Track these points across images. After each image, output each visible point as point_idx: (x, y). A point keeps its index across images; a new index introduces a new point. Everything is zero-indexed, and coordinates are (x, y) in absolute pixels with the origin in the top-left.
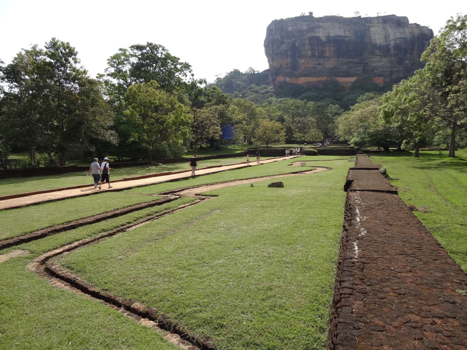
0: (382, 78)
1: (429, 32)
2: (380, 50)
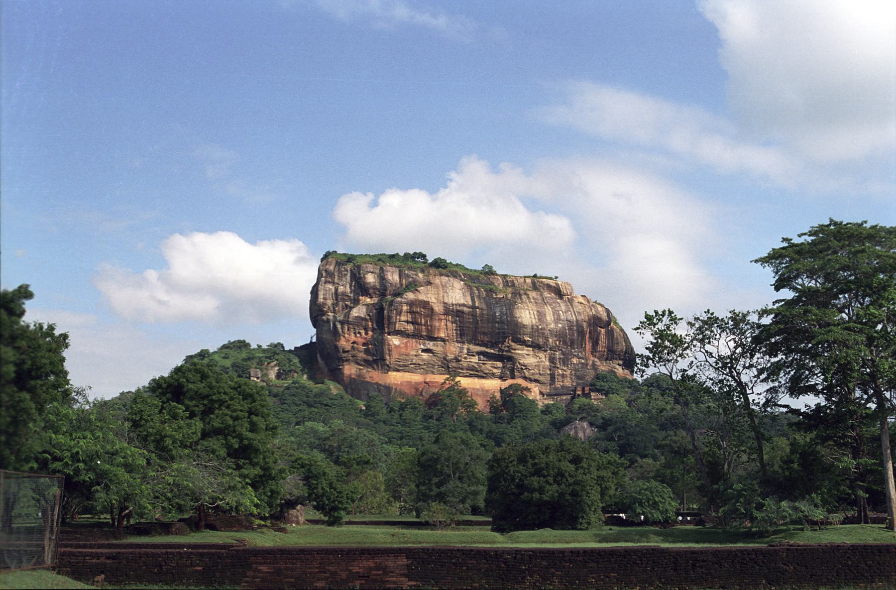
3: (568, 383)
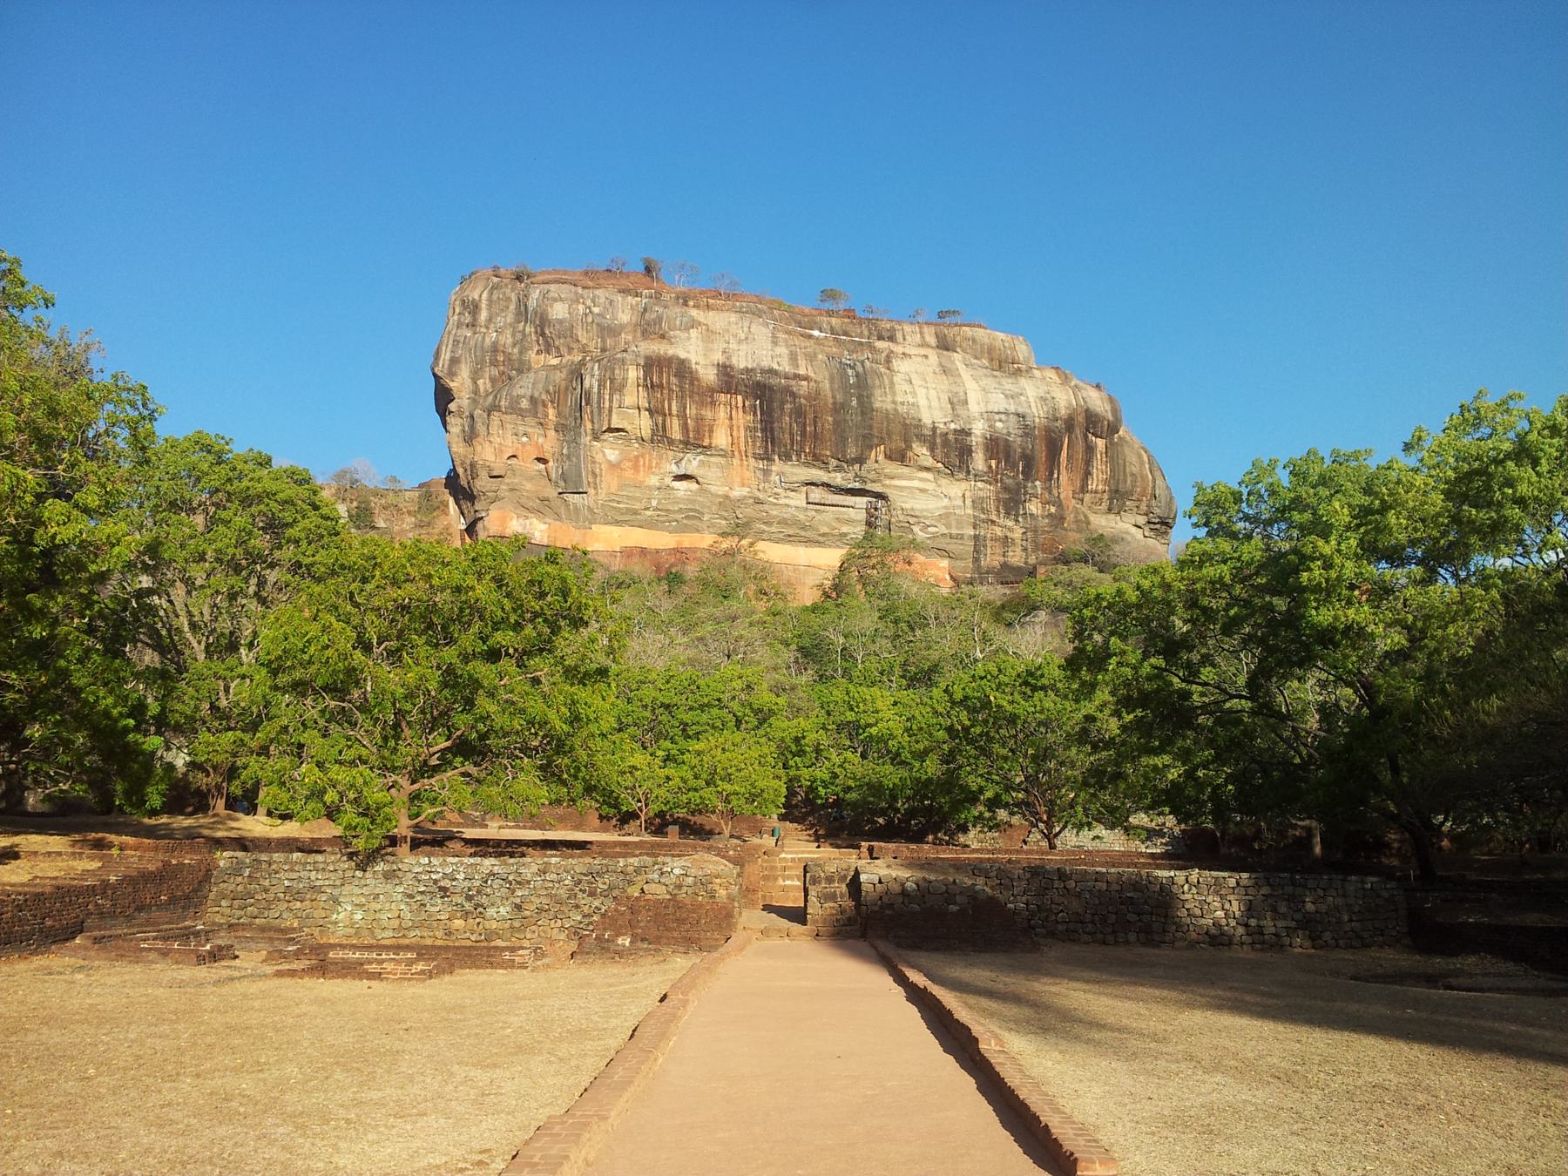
0: (945, 563)
1: (1108, 407)
2: (932, 449)
3: (1016, 558)
